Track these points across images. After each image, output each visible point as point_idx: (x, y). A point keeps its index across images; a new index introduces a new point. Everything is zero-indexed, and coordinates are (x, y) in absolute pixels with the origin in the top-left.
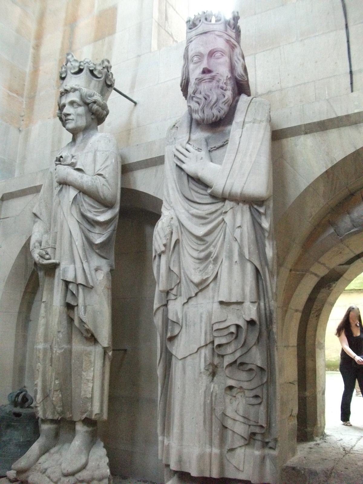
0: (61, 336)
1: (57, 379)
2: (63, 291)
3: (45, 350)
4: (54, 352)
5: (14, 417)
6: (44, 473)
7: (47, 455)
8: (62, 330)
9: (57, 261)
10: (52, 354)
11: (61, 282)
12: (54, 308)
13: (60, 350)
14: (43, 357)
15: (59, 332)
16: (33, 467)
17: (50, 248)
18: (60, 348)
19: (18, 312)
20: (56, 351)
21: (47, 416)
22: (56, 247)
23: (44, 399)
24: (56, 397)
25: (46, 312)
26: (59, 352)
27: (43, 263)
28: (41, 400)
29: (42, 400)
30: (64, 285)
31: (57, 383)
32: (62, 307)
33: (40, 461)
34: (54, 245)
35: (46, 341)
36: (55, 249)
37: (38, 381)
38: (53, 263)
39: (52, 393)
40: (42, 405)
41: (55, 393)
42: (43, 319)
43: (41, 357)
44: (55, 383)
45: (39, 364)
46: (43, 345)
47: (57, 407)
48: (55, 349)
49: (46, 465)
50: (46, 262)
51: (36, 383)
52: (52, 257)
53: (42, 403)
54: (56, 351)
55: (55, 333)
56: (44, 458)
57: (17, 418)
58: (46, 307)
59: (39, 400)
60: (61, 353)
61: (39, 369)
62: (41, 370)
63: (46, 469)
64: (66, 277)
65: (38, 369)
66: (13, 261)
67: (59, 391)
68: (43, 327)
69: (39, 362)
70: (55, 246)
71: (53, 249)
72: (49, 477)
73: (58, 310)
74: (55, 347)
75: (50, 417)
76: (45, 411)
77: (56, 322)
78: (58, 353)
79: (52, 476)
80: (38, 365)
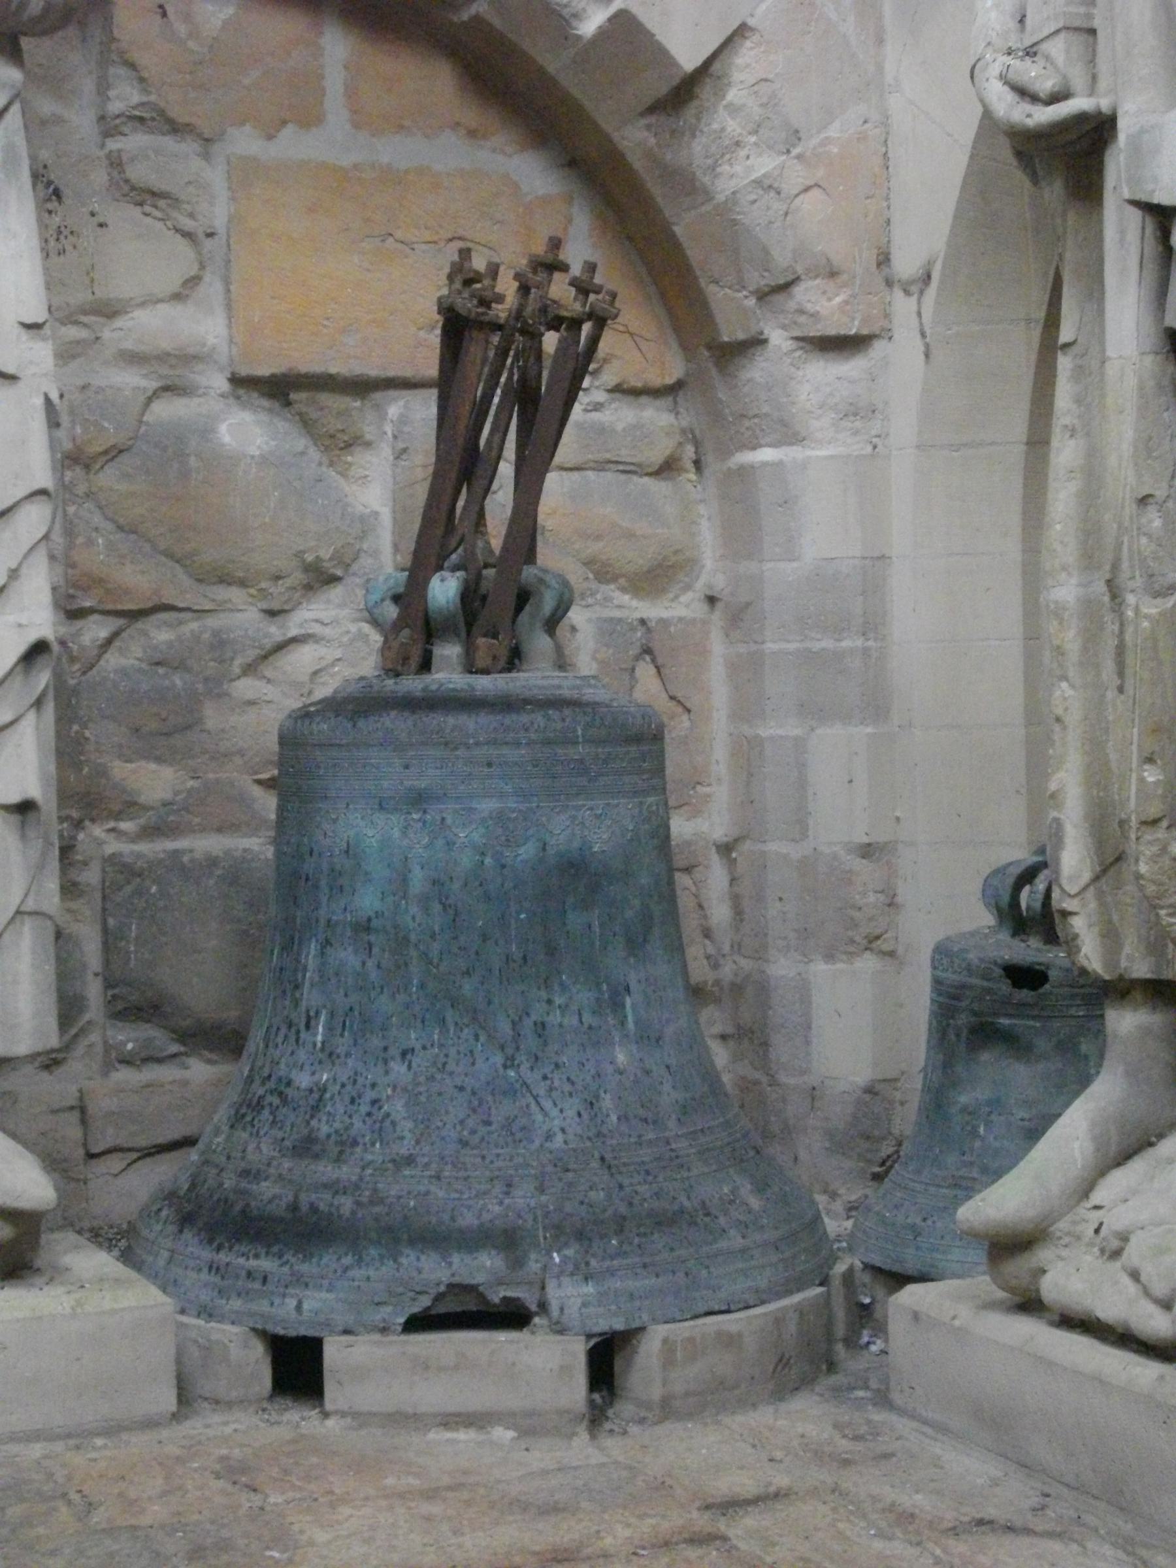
0: (1157, 523)
1: (1150, 760)
2: (1151, 267)
3: (1088, 606)
4: (1130, 613)
5: (1005, 987)
6: (1116, 1254)
7: (1137, 1166)
8: (1160, 493)
9: (1105, 104)
10: (1122, 625)
11: (1135, 216)
12: (1111, 370)
13: (1159, 601)
14: (1085, 649)
15: (1144, 501)
16: (1063, 1225)
17: (1062, 35)
18: (1157, 587)
19: (1024, 438)
20: (1137, 610)
21: (1124, 963)
22: (1097, 23)
23: (1104, 871)
24: (1154, 859)
25: (1078, 401)
26: (1152, 608)
27: (1030, 123)
28: (1087, 876)
29: (1096, 878)
30: (1149, 230)
31: (1151, 779)
32: (1149, 360)
33: (1100, 1195)
34: (1082, 10)
35: (1089, 559)
36: (1092, 32)
37: (1061, 775)
38: (1081, 118)
39: (1133, 836)
40: (1093, 905)
41: (1148, 837)
42: (1072, 442)
43: (1068, 646)
44: (1142, 780)
45: (1064, 685)
46: (1079, 585)
47: (1163, 912)
48: (1131, 599)
49: (1115, 1220)
50: (1044, 115)
51: (1053, 786)
52: (1078, 81)
53: (1090, 894)
54: (1137, 610)
55: (1127, 511)
56: (1119, 1180)
57: (1025, 991)
58: (1079, 372)
59: (1070, 878)
60: (1160, 614)
61: (1066, 709)
62: (1074, 718)
63: (1124, 1238)
64: (1150, 187)
65: (1059, 711)
66: (961, 159)
67: (1165, 824)
68: (1073, 487)
69: (1064, 678)
70: (1089, 16)
71: (1078, 39)
72: (1135, 1275)
73: (1131, 382)
74: (1131, 584)
75: (1142, 969)
76: (1110, 936)
77: (1126, 448)
78: (1146, 617)
79: (1148, 1271)
80: (1058, 693)
